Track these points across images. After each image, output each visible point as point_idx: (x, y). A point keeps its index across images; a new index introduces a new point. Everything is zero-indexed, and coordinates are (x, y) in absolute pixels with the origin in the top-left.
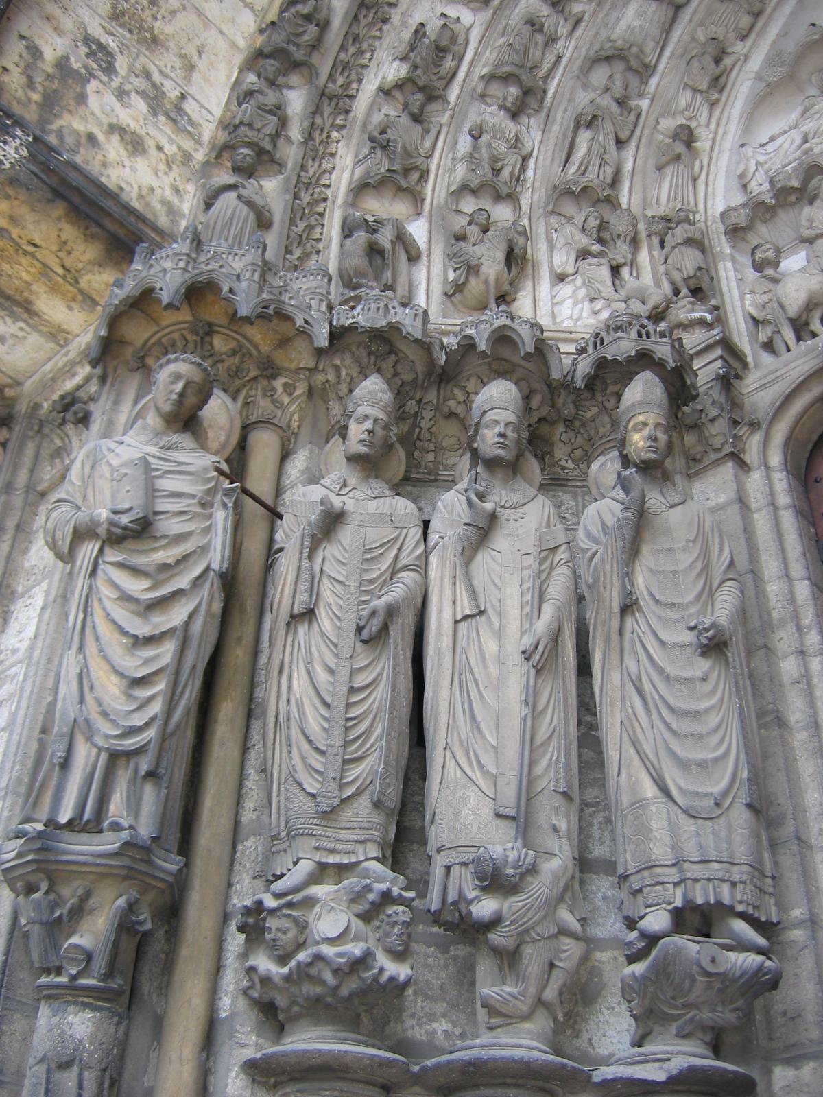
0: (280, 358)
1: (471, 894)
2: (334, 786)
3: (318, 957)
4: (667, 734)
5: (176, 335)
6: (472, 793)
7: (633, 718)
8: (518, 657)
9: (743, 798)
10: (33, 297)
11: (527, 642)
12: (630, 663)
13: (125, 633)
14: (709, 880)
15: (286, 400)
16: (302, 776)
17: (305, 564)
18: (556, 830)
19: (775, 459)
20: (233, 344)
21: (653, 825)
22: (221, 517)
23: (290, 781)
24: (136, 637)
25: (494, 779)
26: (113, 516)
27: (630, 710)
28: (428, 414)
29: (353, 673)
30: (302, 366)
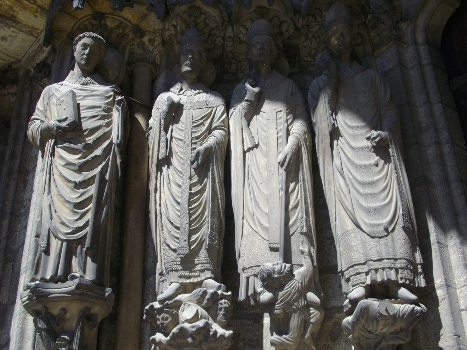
0: (143, 25)
1: (259, 289)
2: (186, 243)
3: (182, 330)
4: (357, 196)
5: (87, 23)
6: (257, 239)
7: (339, 189)
8: (277, 166)
9: (401, 223)
10: (15, 14)
11: (281, 157)
12: (337, 161)
13: (70, 182)
14: (383, 269)
15: (151, 48)
16: (169, 241)
17: (163, 133)
18: (303, 253)
19: (420, 38)
20: (117, 23)
21: (353, 244)
22: (116, 116)
23: (164, 244)
24: (75, 183)
25: (266, 229)
26: (58, 123)
27: (338, 186)
28: (229, 44)
29: (191, 186)
30: (156, 28)
